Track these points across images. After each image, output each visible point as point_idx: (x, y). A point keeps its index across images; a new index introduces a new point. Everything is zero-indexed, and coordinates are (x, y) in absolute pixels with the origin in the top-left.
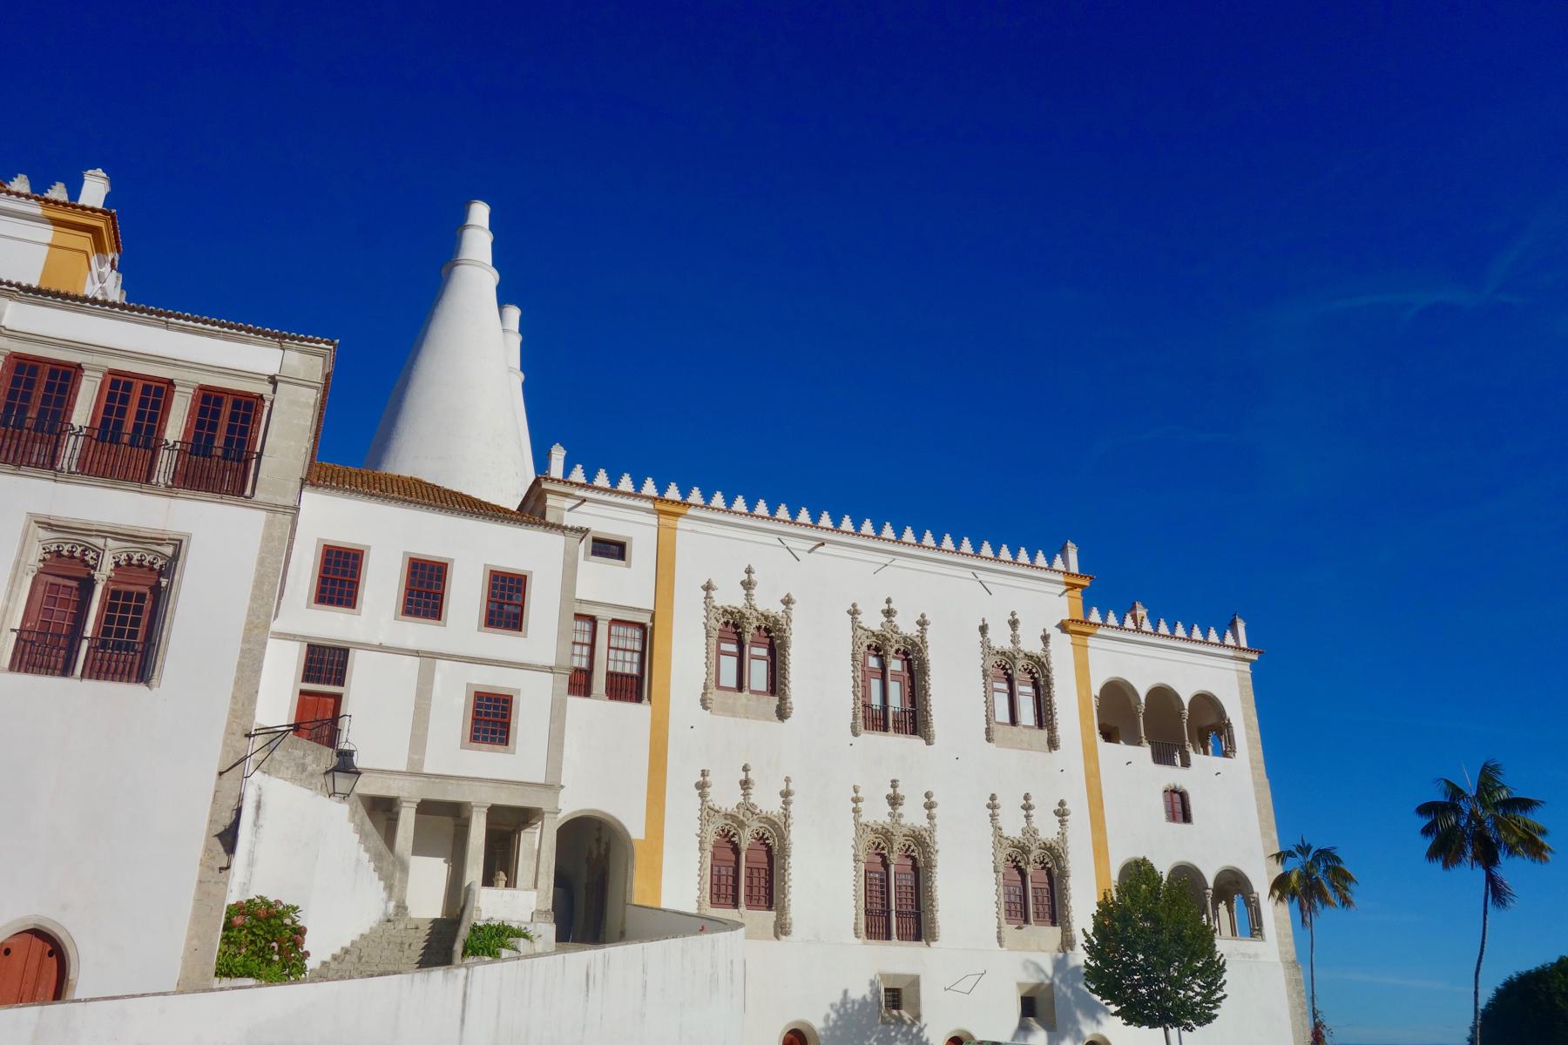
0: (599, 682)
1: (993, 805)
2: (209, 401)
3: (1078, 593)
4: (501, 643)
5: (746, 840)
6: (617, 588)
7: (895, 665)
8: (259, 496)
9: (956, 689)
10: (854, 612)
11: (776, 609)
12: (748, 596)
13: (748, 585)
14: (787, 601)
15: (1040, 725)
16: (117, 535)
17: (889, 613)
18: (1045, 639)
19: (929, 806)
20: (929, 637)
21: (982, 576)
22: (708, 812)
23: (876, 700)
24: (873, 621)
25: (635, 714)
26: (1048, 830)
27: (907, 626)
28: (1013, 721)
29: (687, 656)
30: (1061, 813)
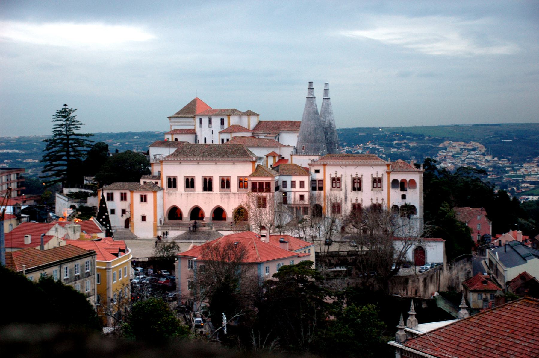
0: (317, 188)
2: (266, 183)
4: (302, 190)
5: (336, 206)
6: (318, 176)
9: (367, 184)
10: (351, 175)
13: (336, 174)
14: (342, 175)
20: (363, 177)
24: (354, 176)
25: (322, 192)
26: (380, 202)
27: (359, 176)
29: (328, 184)
30: (383, 200)
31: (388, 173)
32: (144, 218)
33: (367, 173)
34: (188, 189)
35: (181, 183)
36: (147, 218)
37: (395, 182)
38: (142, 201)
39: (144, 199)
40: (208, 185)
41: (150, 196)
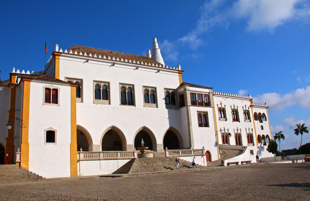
1: (246, 130)
3: (251, 101)
7: (235, 113)
8: (212, 106)
10: (231, 107)
11: (224, 107)
12: (221, 106)
13: (221, 104)
14: (225, 106)
15: (248, 119)
16: (202, 112)
17: (234, 106)
18: (249, 108)
19: (241, 130)
21: (242, 100)
22: (222, 133)
23: (233, 118)
24: (233, 107)
26: (251, 132)
28: (246, 119)
30: (252, 130)
31: (251, 106)
32: (51, 137)
33: (241, 105)
34: (99, 101)
35: (88, 91)
36: (58, 137)
37: (255, 113)
38: (47, 100)
39: (52, 97)
40: (128, 97)
41: (65, 93)
